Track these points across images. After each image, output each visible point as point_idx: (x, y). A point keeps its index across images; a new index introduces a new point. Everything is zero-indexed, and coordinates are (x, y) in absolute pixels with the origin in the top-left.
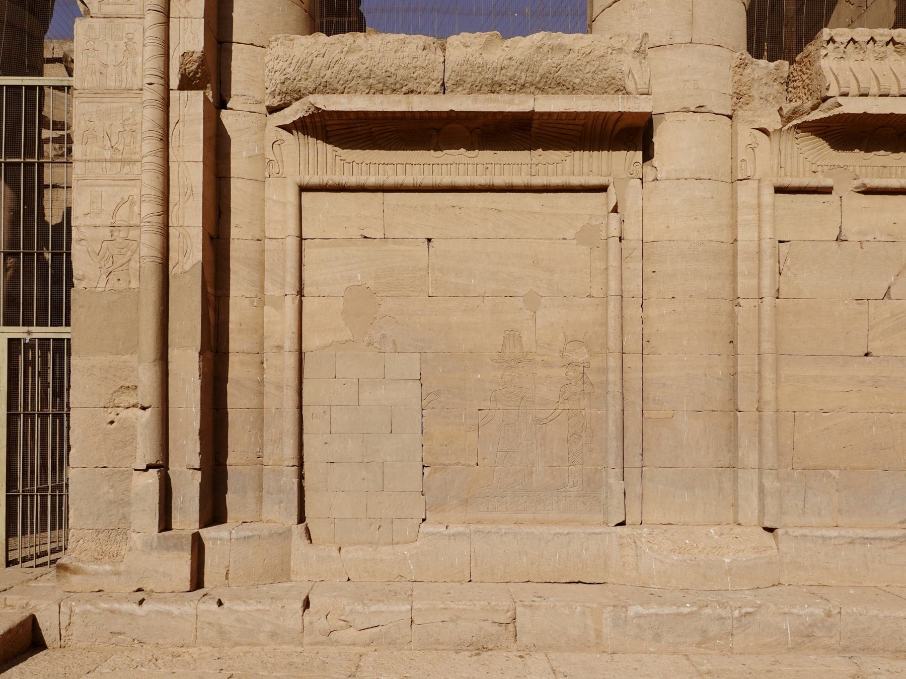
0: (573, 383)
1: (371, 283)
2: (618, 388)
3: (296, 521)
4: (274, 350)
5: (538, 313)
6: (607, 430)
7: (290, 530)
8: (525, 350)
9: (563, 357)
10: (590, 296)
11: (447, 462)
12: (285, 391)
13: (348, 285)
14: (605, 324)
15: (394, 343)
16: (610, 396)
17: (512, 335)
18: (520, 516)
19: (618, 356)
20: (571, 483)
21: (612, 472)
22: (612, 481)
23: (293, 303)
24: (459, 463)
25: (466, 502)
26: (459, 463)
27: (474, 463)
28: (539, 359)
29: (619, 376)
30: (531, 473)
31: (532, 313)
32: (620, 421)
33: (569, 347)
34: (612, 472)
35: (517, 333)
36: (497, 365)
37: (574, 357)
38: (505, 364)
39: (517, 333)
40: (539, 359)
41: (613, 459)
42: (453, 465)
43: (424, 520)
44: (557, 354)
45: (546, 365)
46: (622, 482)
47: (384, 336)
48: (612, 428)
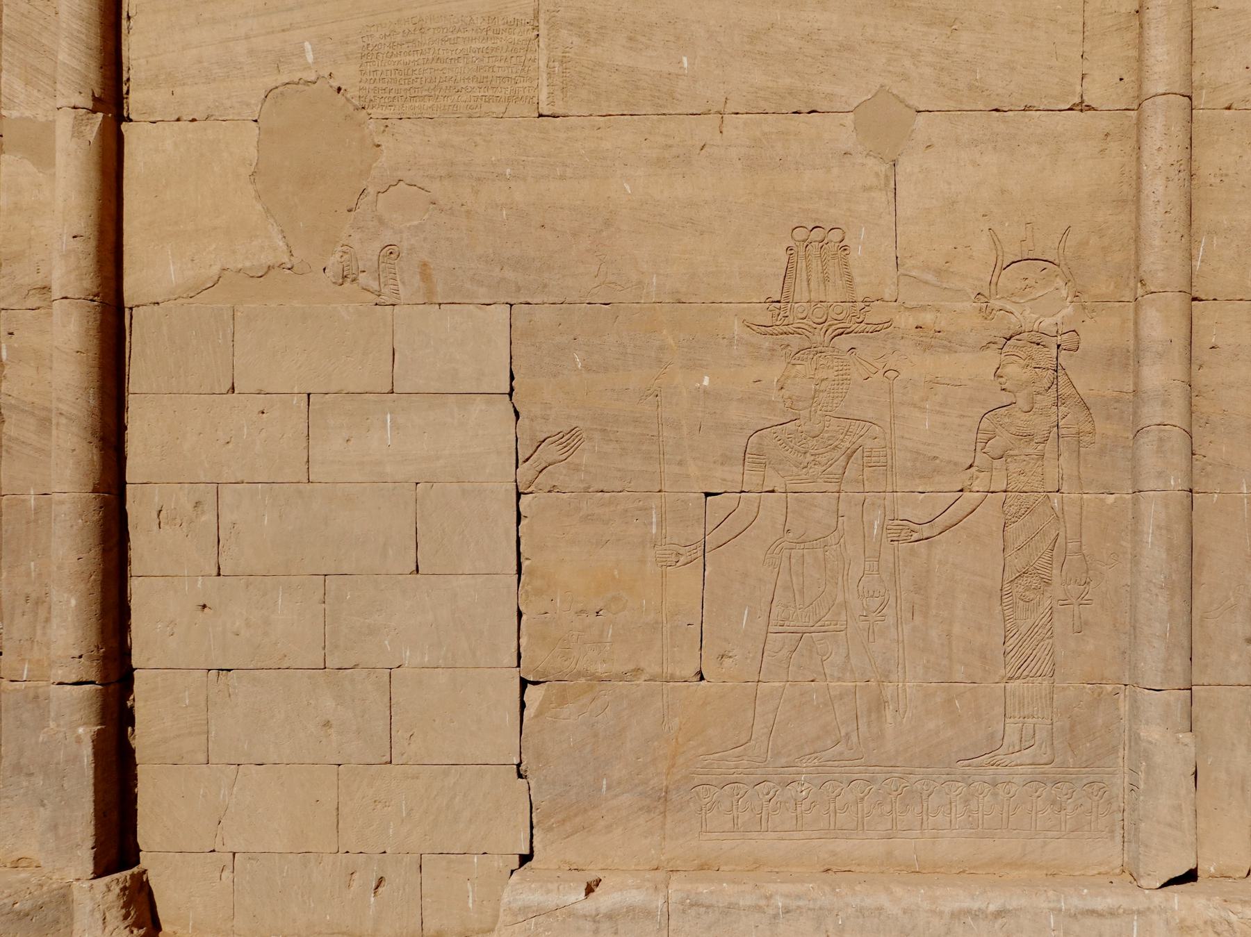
0: (1022, 403)
1: (347, 74)
2: (1176, 414)
3: (89, 867)
4: (33, 301)
5: (905, 166)
6: (1136, 560)
7: (64, 898)
8: (860, 293)
9: (987, 313)
10: (1082, 106)
11: (600, 669)
12: (54, 432)
13: (270, 81)
14: (1135, 201)
15: (425, 272)
16: (1147, 445)
17: (818, 242)
18: (841, 846)
19: (1177, 302)
20: (1012, 737)
21: (1153, 704)
22: (1153, 733)
23: (77, 133)
24: (638, 670)
25: (661, 802)
26: (638, 670)
27: (690, 670)
28: (905, 321)
29: (1179, 371)
30: (879, 705)
31: (884, 168)
32: (1180, 528)
33: (1008, 280)
34: (1153, 704)
35: (835, 236)
36: (766, 343)
37: (1025, 316)
38: (795, 341)
39: (835, 236)
40: (905, 321)
41: (1153, 660)
42: (622, 677)
43: (525, 859)
44: (968, 305)
45: (931, 339)
46: (1186, 738)
47: (390, 251)
48: (1155, 555)
